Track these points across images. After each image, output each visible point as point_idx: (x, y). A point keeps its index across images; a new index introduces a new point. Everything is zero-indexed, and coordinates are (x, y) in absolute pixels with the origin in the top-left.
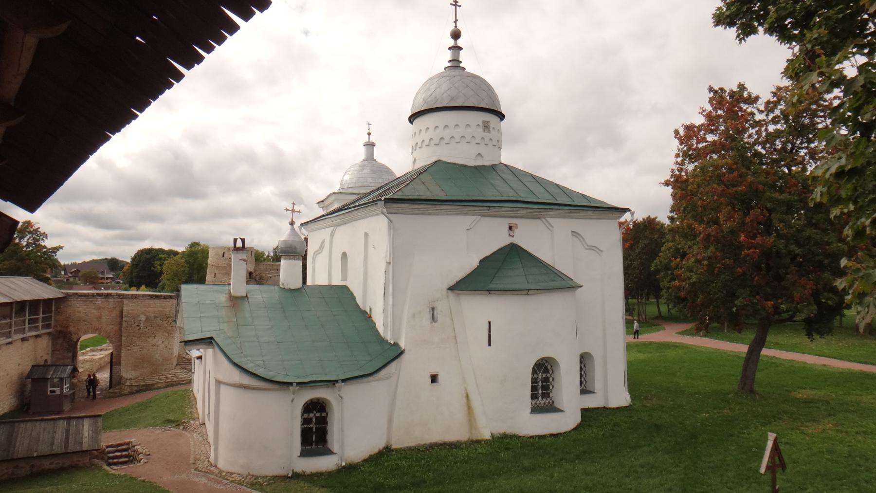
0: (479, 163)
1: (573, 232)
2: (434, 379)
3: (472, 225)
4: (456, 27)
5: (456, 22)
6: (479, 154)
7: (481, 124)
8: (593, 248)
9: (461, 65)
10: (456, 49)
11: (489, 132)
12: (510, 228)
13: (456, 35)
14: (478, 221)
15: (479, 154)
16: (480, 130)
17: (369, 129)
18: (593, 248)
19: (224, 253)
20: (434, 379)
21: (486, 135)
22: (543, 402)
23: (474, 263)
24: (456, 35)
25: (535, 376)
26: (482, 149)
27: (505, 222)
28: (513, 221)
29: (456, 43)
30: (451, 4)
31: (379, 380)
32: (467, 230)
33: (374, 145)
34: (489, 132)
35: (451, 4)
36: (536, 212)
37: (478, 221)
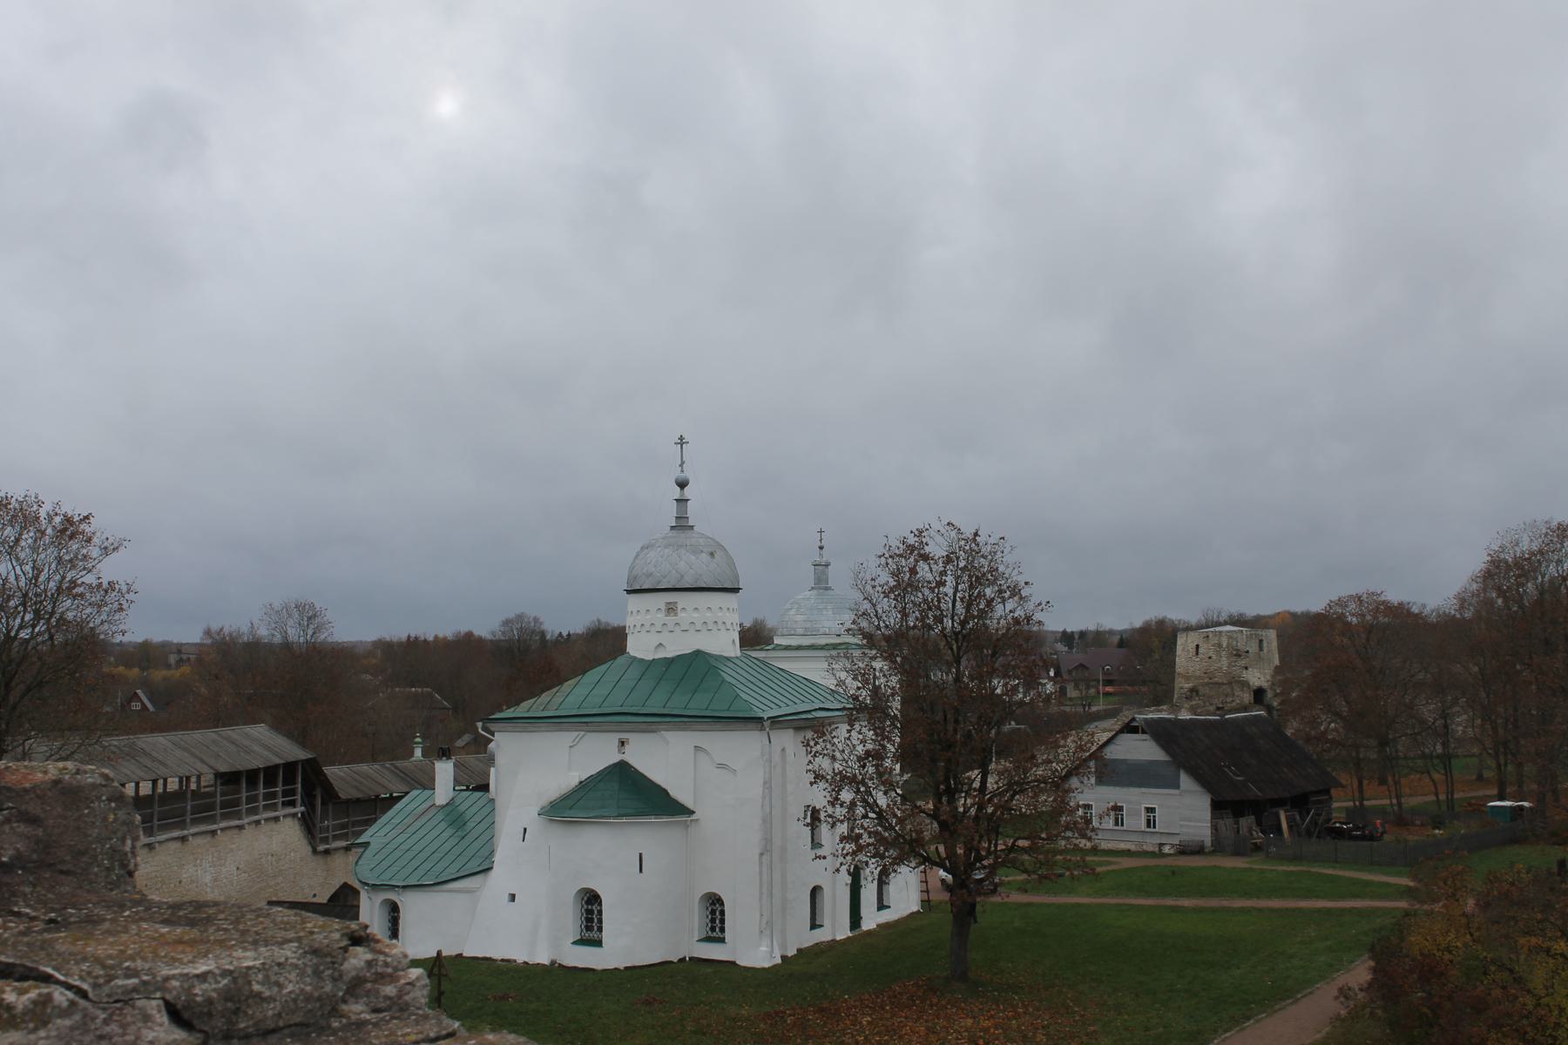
0: (660, 655)
1: (695, 747)
2: (513, 897)
3: (577, 740)
4: (682, 471)
5: (681, 465)
6: (661, 644)
7: (663, 607)
8: (721, 766)
9: (690, 524)
10: (682, 502)
11: (676, 615)
12: (622, 743)
13: (682, 485)
14: (581, 738)
15: (661, 644)
16: (661, 615)
17: (821, 540)
18: (721, 766)
19: (1197, 646)
20: (513, 897)
21: (671, 619)
22: (587, 935)
23: (573, 779)
24: (682, 485)
25: (590, 907)
26: (665, 638)
27: (612, 739)
28: (624, 736)
29: (682, 495)
30: (675, 443)
31: (451, 891)
32: (571, 747)
33: (827, 565)
34: (676, 615)
35: (675, 443)
36: (644, 726)
37: (581, 738)
